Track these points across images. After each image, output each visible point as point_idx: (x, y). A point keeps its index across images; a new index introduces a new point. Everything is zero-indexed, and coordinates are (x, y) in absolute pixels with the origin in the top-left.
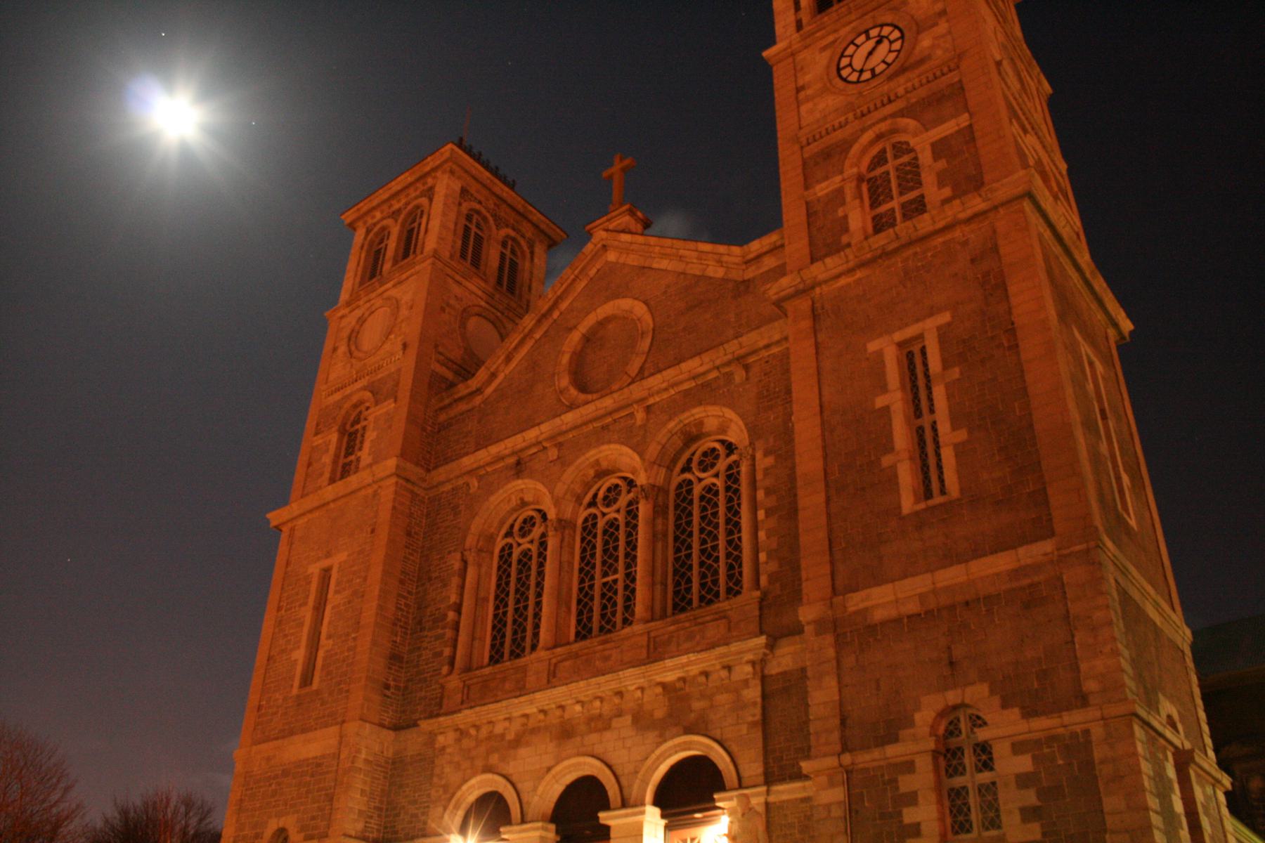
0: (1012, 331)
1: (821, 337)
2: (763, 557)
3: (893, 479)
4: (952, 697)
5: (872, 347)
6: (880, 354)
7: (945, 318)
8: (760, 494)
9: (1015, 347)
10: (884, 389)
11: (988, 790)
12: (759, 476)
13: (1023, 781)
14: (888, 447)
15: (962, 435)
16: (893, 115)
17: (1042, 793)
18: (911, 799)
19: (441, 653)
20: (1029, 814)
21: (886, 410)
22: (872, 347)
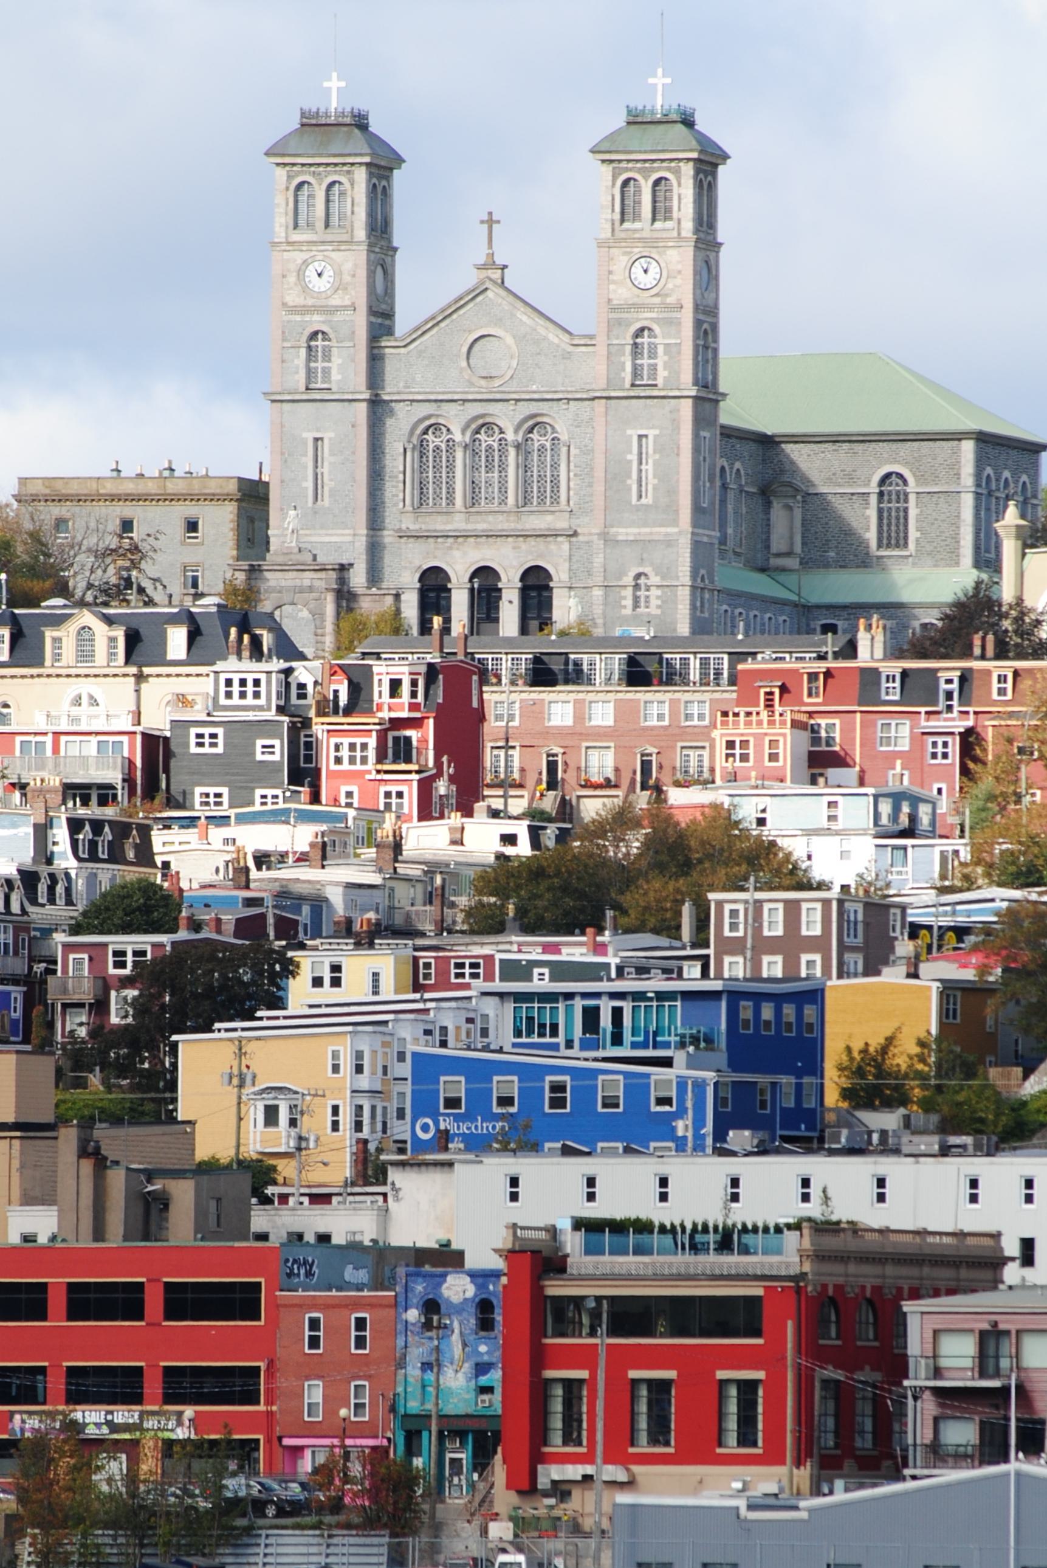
0: (678, 448)
1: (609, 418)
2: (572, 493)
3: (630, 489)
4: (641, 570)
5: (629, 432)
6: (631, 436)
7: (657, 432)
8: (572, 464)
9: (678, 455)
10: (631, 452)
11: (647, 597)
12: (572, 458)
13: (658, 597)
14: (630, 477)
15: (656, 481)
16: (652, 319)
17: (663, 602)
18: (625, 598)
19: (397, 496)
20: (659, 607)
21: (630, 461)
22: (629, 432)
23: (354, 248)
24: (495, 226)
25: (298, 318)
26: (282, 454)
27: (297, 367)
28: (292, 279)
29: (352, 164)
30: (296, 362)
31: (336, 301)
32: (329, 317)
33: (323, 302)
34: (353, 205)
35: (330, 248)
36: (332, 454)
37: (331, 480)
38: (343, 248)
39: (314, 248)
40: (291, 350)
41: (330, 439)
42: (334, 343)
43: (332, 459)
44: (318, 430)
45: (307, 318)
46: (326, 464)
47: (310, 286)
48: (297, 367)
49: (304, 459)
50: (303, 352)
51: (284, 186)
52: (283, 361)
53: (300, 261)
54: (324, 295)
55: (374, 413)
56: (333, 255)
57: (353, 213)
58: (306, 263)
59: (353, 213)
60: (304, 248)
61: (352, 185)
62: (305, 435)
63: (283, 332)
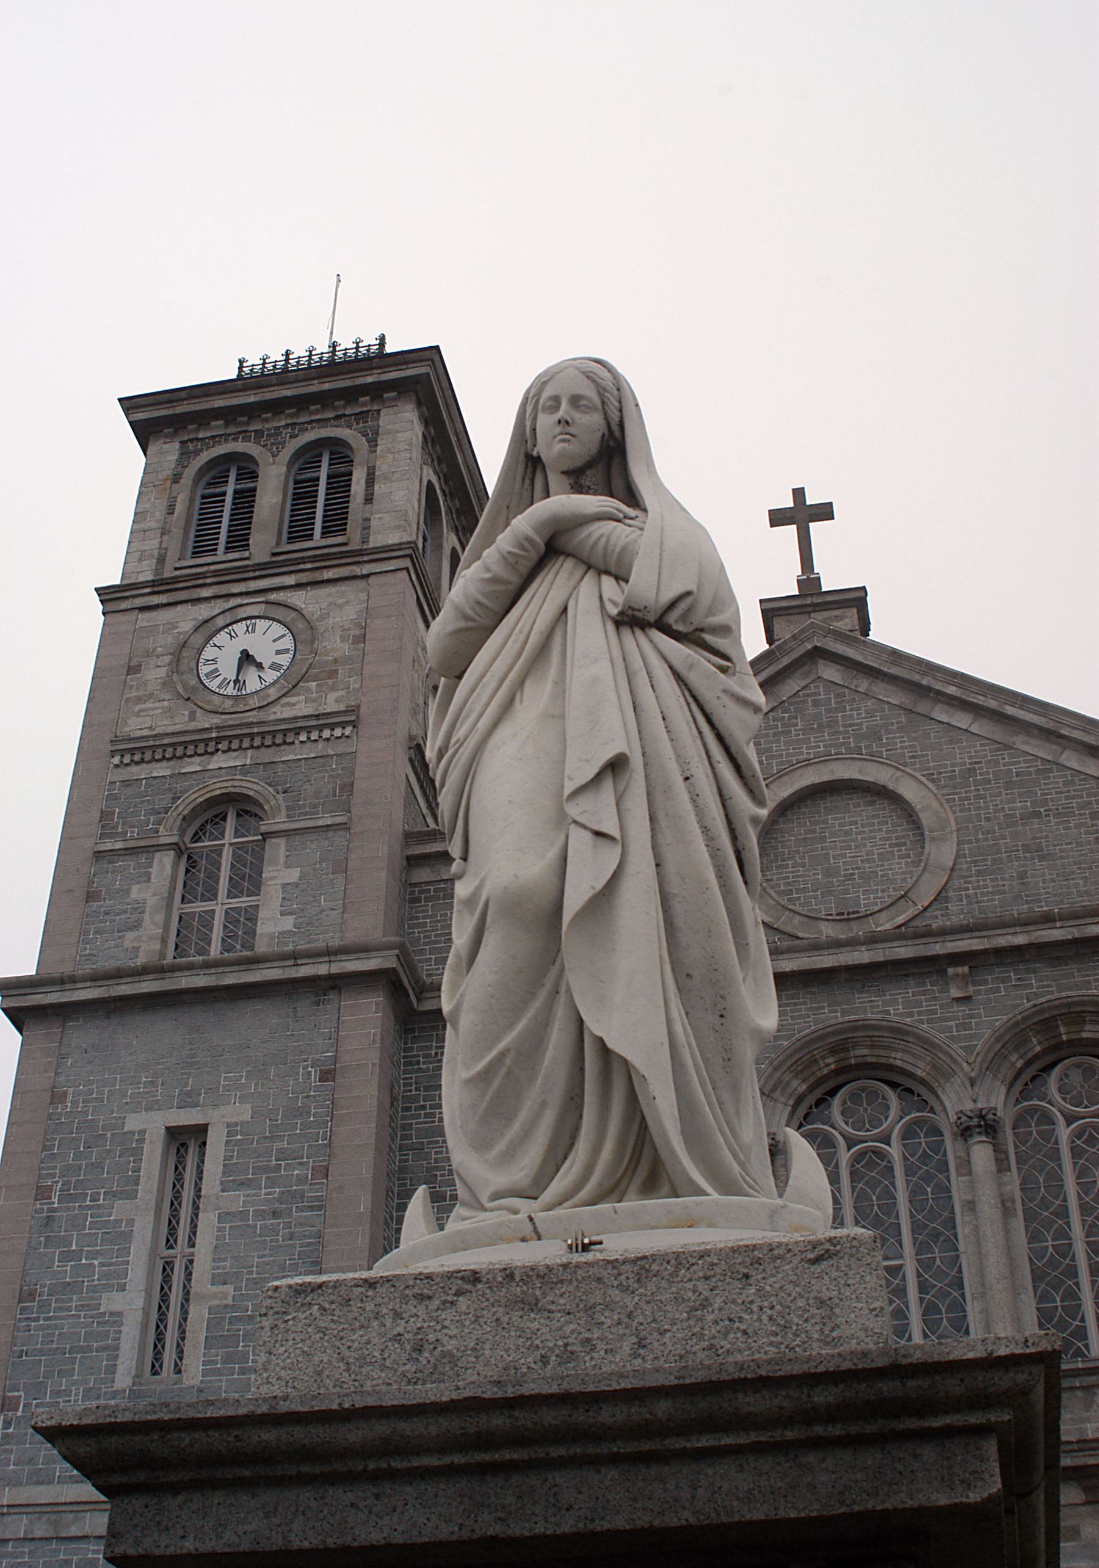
23: (366, 569)
24: (816, 528)
25: (161, 770)
26: (42, 1193)
27: (139, 908)
28: (155, 673)
29: (377, 391)
30: (135, 893)
31: (299, 706)
32: (266, 755)
33: (252, 717)
34: (370, 481)
35: (290, 580)
36: (233, 1179)
37: (219, 1279)
38: (328, 574)
39: (236, 588)
40: (130, 863)
41: (231, 1128)
42: (278, 821)
43: (237, 1200)
44: (188, 1101)
45: (193, 765)
46: (207, 1221)
47: (213, 685)
48: (139, 908)
49: (120, 1209)
50: (164, 865)
51: (169, 472)
52: (91, 896)
53: (187, 626)
54: (254, 702)
55: (410, 1063)
56: (297, 598)
57: (369, 499)
58: (207, 629)
59: (369, 499)
60: (205, 593)
61: (373, 443)
62: (133, 1123)
63: (105, 815)
